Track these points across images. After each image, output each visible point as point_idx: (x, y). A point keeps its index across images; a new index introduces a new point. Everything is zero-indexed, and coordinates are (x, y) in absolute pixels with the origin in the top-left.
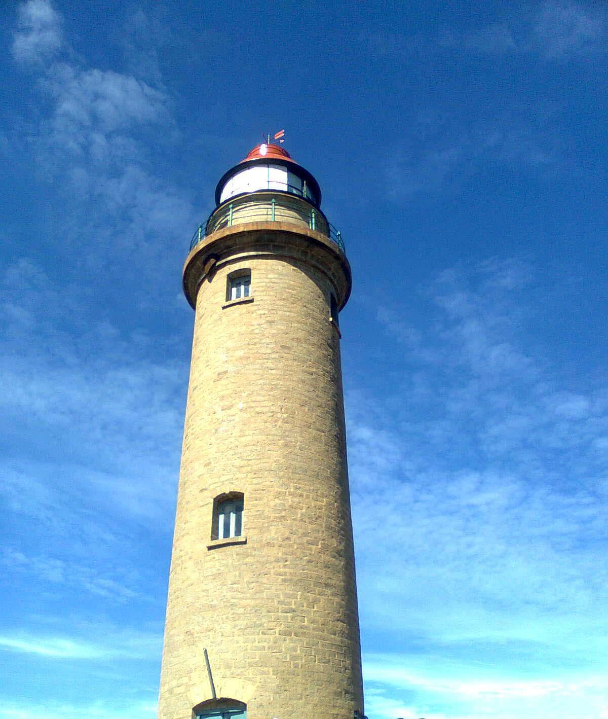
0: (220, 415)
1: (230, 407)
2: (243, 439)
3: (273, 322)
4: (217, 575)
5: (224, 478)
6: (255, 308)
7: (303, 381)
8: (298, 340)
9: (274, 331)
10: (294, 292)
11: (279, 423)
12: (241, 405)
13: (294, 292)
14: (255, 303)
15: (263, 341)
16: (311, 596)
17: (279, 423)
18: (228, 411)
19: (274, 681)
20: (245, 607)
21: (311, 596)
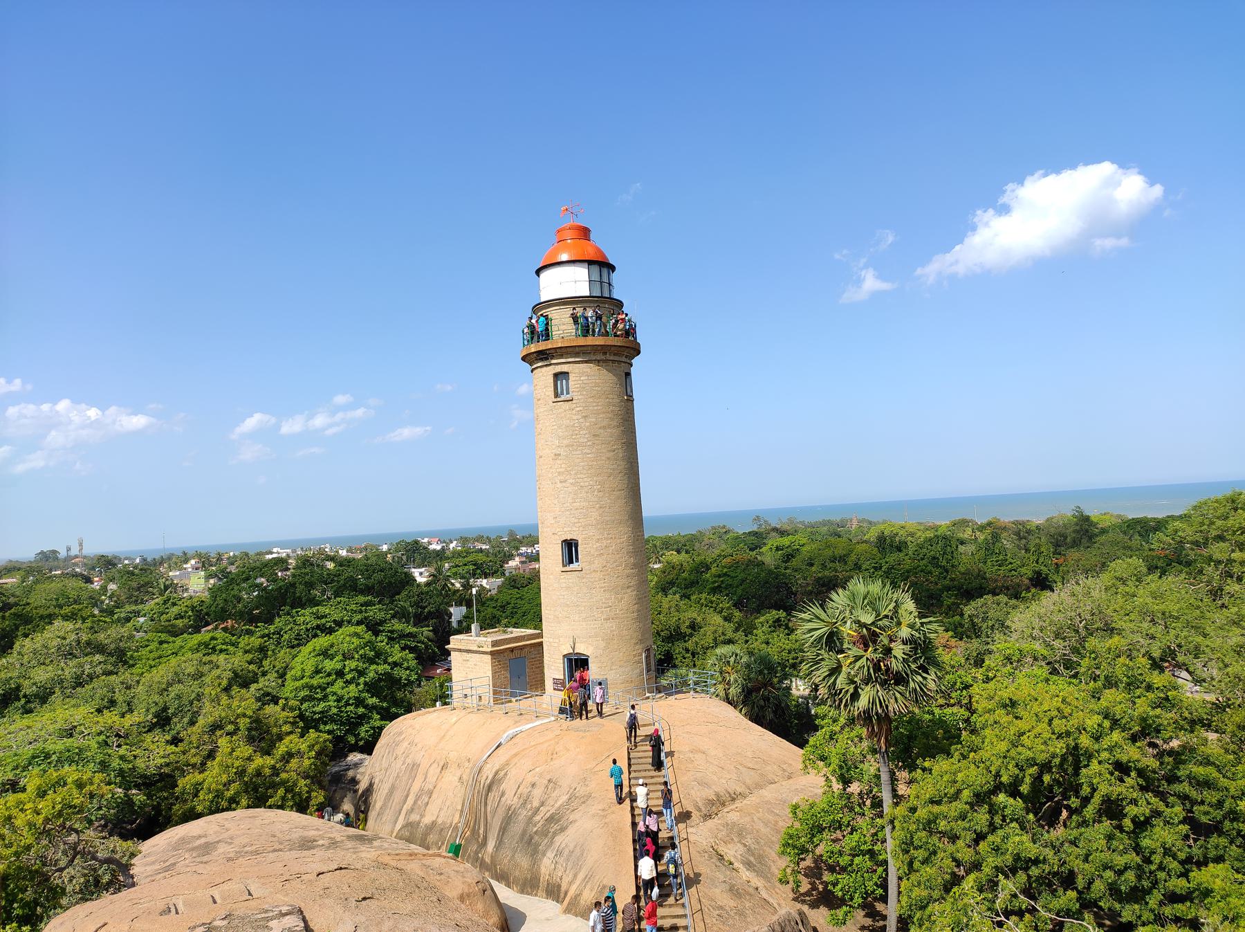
0: (559, 485)
1: (565, 481)
2: (575, 504)
3: (586, 416)
4: (568, 588)
5: (565, 529)
6: (574, 405)
7: (608, 459)
8: (604, 428)
9: (587, 424)
10: (599, 389)
11: (596, 493)
12: (571, 481)
13: (599, 389)
14: (574, 402)
15: (581, 432)
16: (619, 596)
17: (596, 493)
18: (564, 484)
19: (602, 644)
20: (585, 607)
21: (619, 596)
